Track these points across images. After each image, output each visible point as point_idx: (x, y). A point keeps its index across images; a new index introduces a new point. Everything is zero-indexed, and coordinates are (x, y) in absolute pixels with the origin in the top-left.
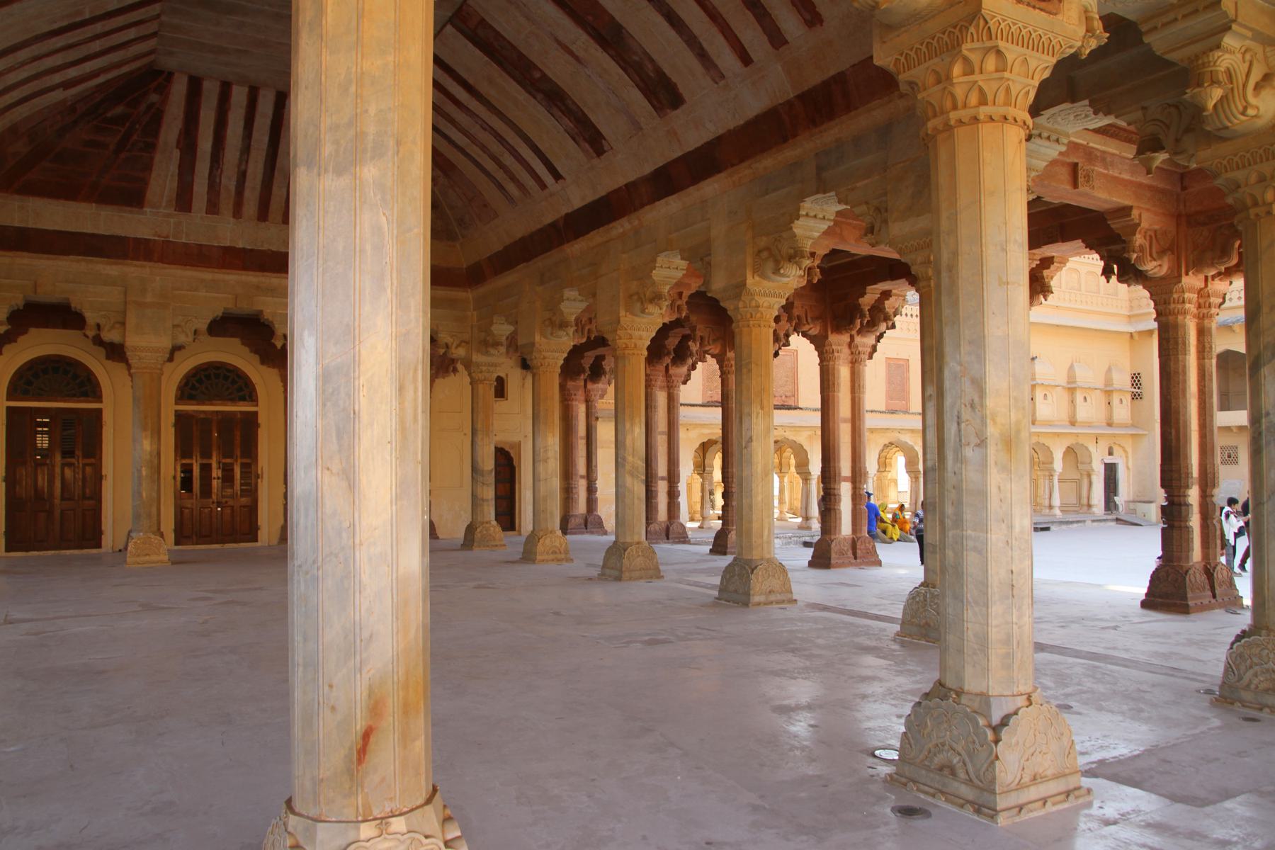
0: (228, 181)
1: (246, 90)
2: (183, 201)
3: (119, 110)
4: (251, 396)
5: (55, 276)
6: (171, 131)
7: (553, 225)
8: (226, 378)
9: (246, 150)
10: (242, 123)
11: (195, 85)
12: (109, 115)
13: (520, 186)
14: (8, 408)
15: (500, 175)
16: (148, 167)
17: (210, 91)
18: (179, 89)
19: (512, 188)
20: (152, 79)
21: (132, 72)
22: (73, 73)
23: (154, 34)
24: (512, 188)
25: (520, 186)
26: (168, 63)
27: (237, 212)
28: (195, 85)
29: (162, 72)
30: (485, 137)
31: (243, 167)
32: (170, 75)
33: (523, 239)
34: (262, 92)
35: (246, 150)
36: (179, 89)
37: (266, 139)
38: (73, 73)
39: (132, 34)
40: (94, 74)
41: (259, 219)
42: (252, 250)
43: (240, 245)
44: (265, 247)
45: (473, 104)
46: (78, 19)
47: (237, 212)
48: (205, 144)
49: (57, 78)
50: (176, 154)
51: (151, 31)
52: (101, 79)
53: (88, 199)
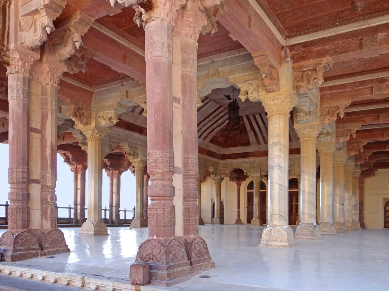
1: (258, 115)
3: (237, 126)
6: (248, 128)
8: (294, 182)
14: (266, 190)
16: (248, 136)
18: (245, 119)
28: (247, 117)
32: (242, 116)
36: (245, 119)
48: (257, 129)
49: (214, 126)
50: (252, 132)
53: (240, 146)
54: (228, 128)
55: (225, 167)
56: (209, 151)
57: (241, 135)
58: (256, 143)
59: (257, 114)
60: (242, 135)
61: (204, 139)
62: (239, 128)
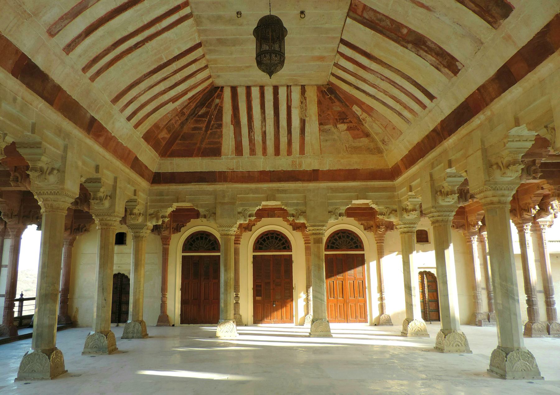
0: (258, 137)
1: (258, 88)
2: (239, 150)
3: (203, 110)
4: (288, 247)
5: (190, 195)
6: (227, 116)
7: (434, 130)
9: (264, 119)
10: (259, 106)
11: (234, 90)
12: (200, 113)
13: (411, 111)
15: (398, 107)
16: (221, 136)
17: (242, 92)
18: (227, 94)
19: (406, 113)
20: (214, 91)
21: (204, 90)
22: (173, 93)
23: (206, 67)
24: (406, 113)
25: (411, 111)
26: (219, 82)
27: (265, 152)
28: (234, 90)
29: (218, 87)
30: (384, 85)
31: (264, 129)
32: (222, 87)
33: (418, 144)
34: (266, 88)
35: (264, 119)
36: (227, 94)
37: (272, 112)
38: (173, 93)
39: (193, 68)
40: (185, 93)
41: (275, 155)
42: (274, 171)
43: (268, 169)
44: (280, 169)
45: (374, 66)
46: (162, 63)
47: (265, 152)
49: (166, 97)
50: (232, 127)
51: (203, 65)
52: (190, 95)
53: (197, 156)
54: (185, 110)
55: (160, 201)
56: (136, 158)
57: (206, 131)
58: (232, 154)
59: (255, 86)
60: (209, 132)
61: (136, 126)
62: (203, 116)
